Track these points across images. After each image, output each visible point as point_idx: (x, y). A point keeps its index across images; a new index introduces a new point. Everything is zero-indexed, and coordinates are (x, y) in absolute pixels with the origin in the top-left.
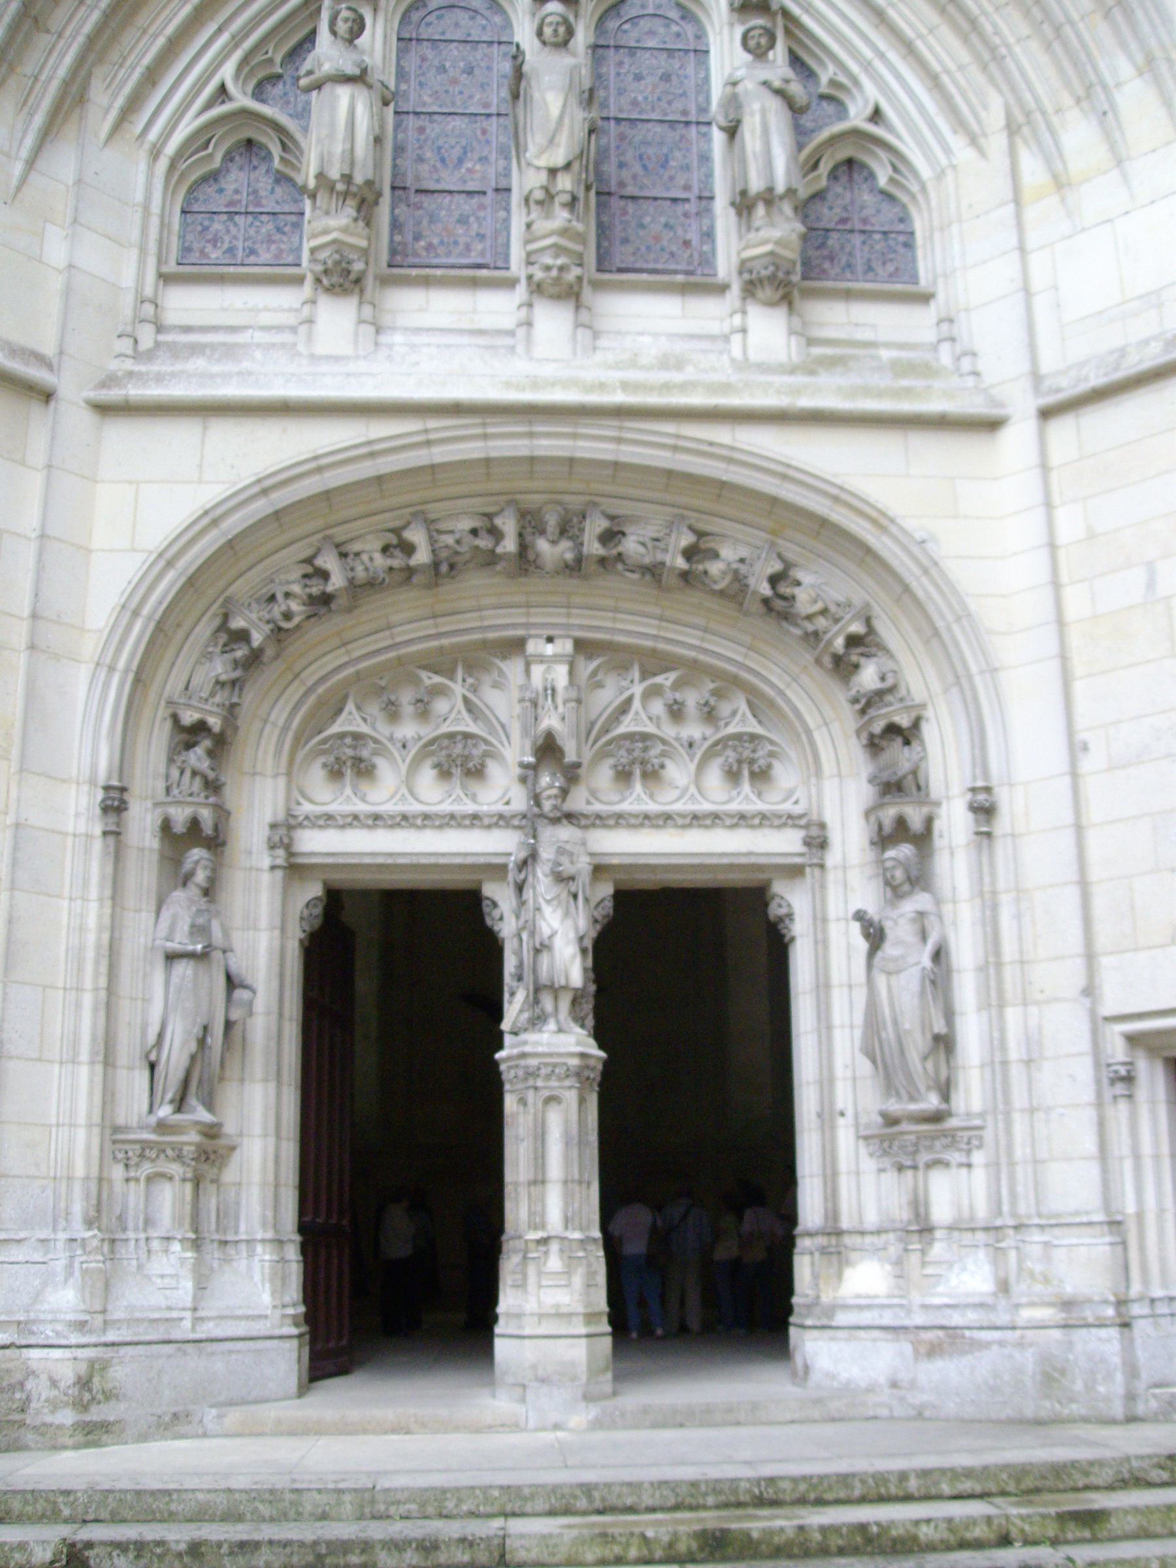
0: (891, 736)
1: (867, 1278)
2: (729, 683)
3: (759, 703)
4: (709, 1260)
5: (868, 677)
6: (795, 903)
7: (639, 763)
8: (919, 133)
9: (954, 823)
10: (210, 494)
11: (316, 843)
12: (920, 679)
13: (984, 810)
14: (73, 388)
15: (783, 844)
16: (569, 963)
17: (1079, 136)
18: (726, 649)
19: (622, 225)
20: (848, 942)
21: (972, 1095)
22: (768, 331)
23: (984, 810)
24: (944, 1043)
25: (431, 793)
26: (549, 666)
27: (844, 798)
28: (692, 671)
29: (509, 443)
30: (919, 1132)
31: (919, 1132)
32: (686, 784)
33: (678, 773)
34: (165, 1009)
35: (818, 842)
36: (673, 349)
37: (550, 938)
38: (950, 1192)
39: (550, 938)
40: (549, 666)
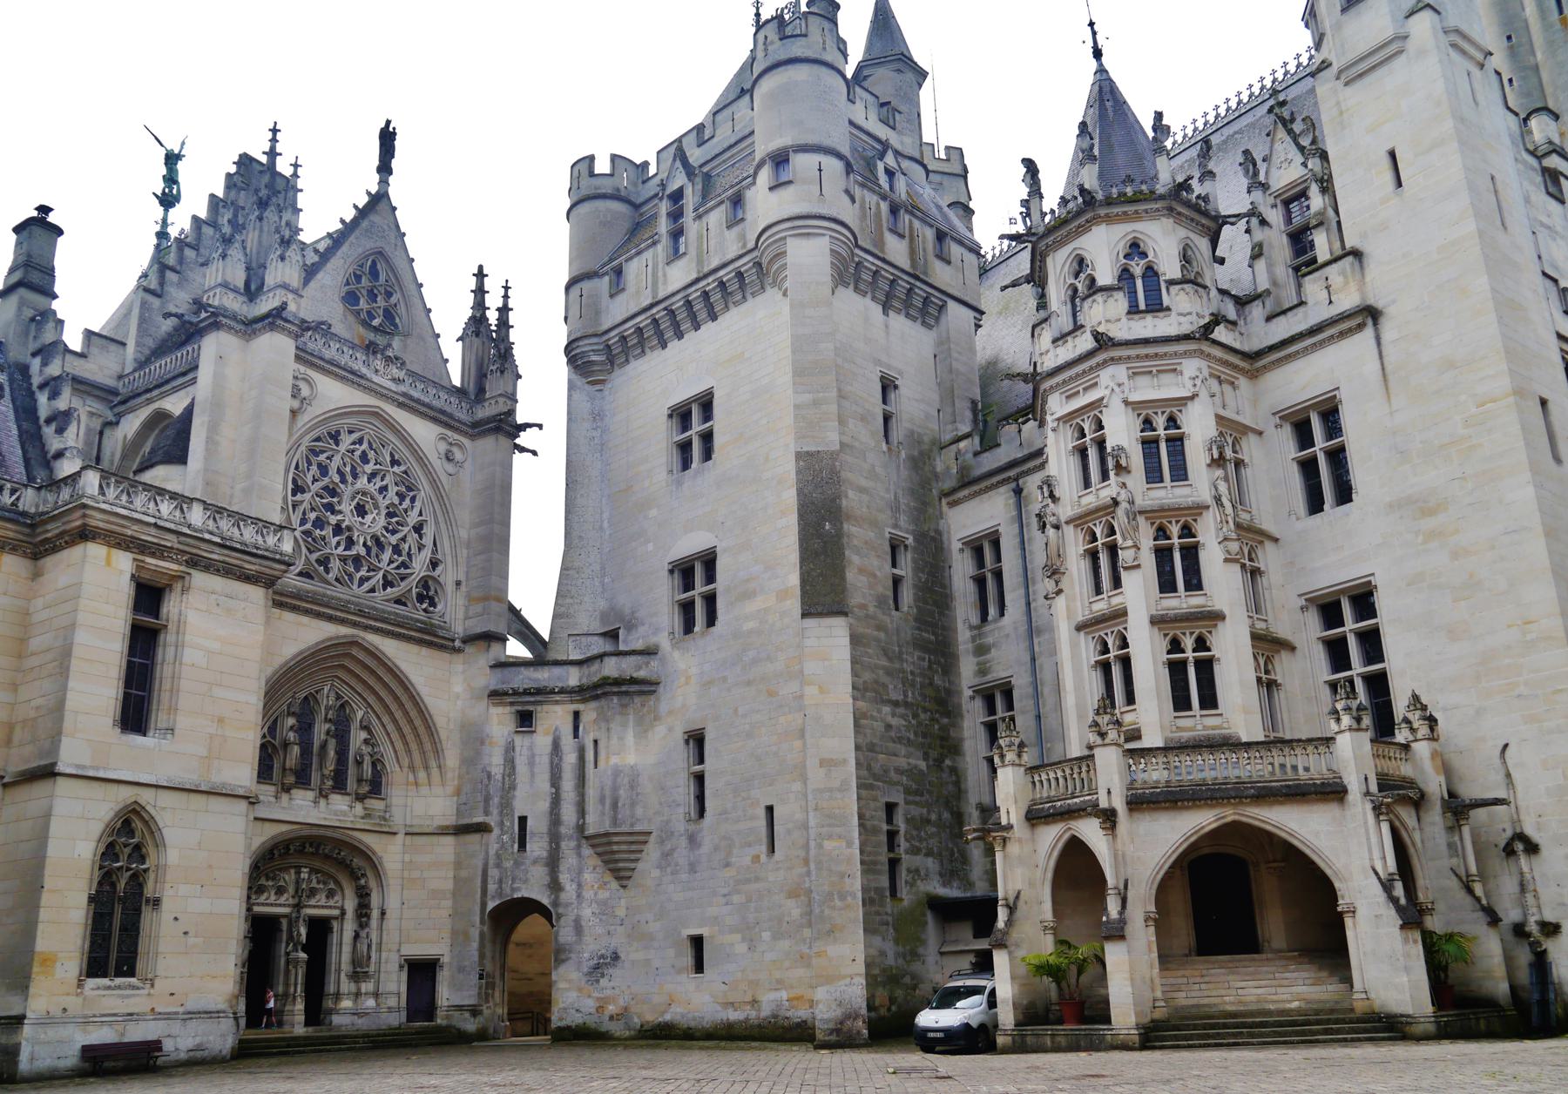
0: (363, 895)
1: (346, 1004)
2: (332, 877)
3: (337, 882)
5: (363, 882)
6: (335, 924)
7: (313, 892)
9: (375, 914)
10: (263, 839)
11: (256, 909)
12: (373, 884)
15: (336, 912)
17: (422, 775)
18: (332, 871)
22: (359, 808)
23: (383, 913)
27: (350, 904)
28: (324, 874)
29: (315, 832)
30: (359, 972)
31: (357, 975)
32: (321, 899)
35: (343, 913)
38: (367, 987)
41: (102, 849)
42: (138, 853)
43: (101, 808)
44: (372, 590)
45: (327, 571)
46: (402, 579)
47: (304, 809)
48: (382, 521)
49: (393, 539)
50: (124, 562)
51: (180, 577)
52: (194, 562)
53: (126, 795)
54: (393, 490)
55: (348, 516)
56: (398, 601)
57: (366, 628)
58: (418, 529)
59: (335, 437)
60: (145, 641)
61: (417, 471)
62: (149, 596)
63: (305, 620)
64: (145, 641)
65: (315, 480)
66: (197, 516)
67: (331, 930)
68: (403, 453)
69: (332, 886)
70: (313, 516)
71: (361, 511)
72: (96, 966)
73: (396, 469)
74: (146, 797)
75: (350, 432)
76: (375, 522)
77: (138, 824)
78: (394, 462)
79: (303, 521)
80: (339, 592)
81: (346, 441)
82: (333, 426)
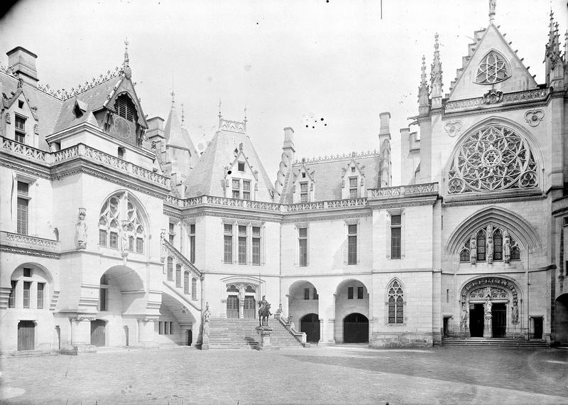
0: (515, 295)
4: (499, 330)
5: (513, 290)
8: (521, 247)
9: (519, 302)
13: (521, 301)
14: (455, 274)
16: (490, 310)
19: (496, 257)
20: (511, 309)
21: (519, 320)
24: (517, 316)
25: (479, 298)
26: (489, 289)
27: (511, 298)
30: (515, 321)
33: (498, 296)
34: (464, 314)
36: (499, 268)
37: (488, 308)
39: (488, 308)
40: (489, 289)
41: (389, 290)
42: (400, 290)
43: (387, 279)
44: (500, 186)
45: (477, 186)
46: (514, 177)
47: (484, 269)
48: (501, 159)
49: (507, 164)
50: (384, 212)
51: (401, 211)
52: (403, 205)
53: (392, 276)
54: (506, 145)
55: (484, 163)
56: (513, 186)
57: (495, 202)
58: (522, 155)
59: (477, 136)
60: (396, 232)
61: (517, 132)
62: (396, 218)
63: (467, 207)
64: (396, 232)
65: (469, 156)
66: (402, 190)
67: (506, 307)
68: (509, 128)
69: (503, 292)
70: (468, 170)
71: (491, 158)
72: (391, 320)
73: (508, 136)
74: (398, 275)
75: (482, 131)
76: (498, 160)
77: (398, 283)
78: (506, 133)
79: (465, 172)
80: (482, 193)
81: (481, 136)
82: (474, 133)
